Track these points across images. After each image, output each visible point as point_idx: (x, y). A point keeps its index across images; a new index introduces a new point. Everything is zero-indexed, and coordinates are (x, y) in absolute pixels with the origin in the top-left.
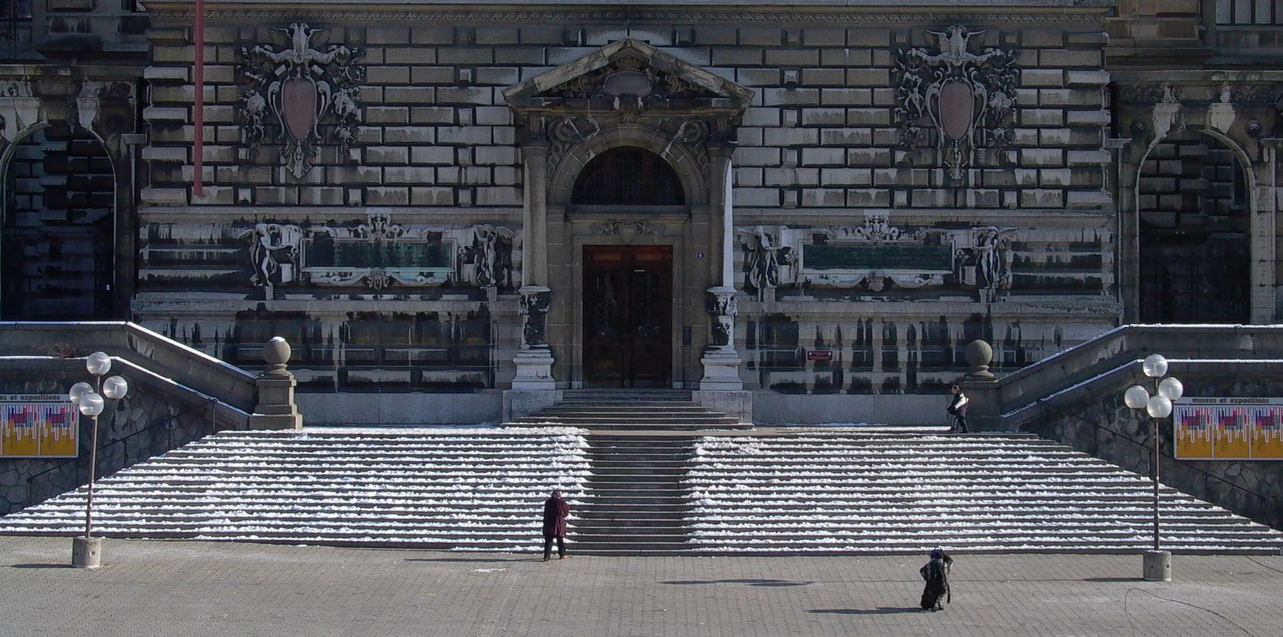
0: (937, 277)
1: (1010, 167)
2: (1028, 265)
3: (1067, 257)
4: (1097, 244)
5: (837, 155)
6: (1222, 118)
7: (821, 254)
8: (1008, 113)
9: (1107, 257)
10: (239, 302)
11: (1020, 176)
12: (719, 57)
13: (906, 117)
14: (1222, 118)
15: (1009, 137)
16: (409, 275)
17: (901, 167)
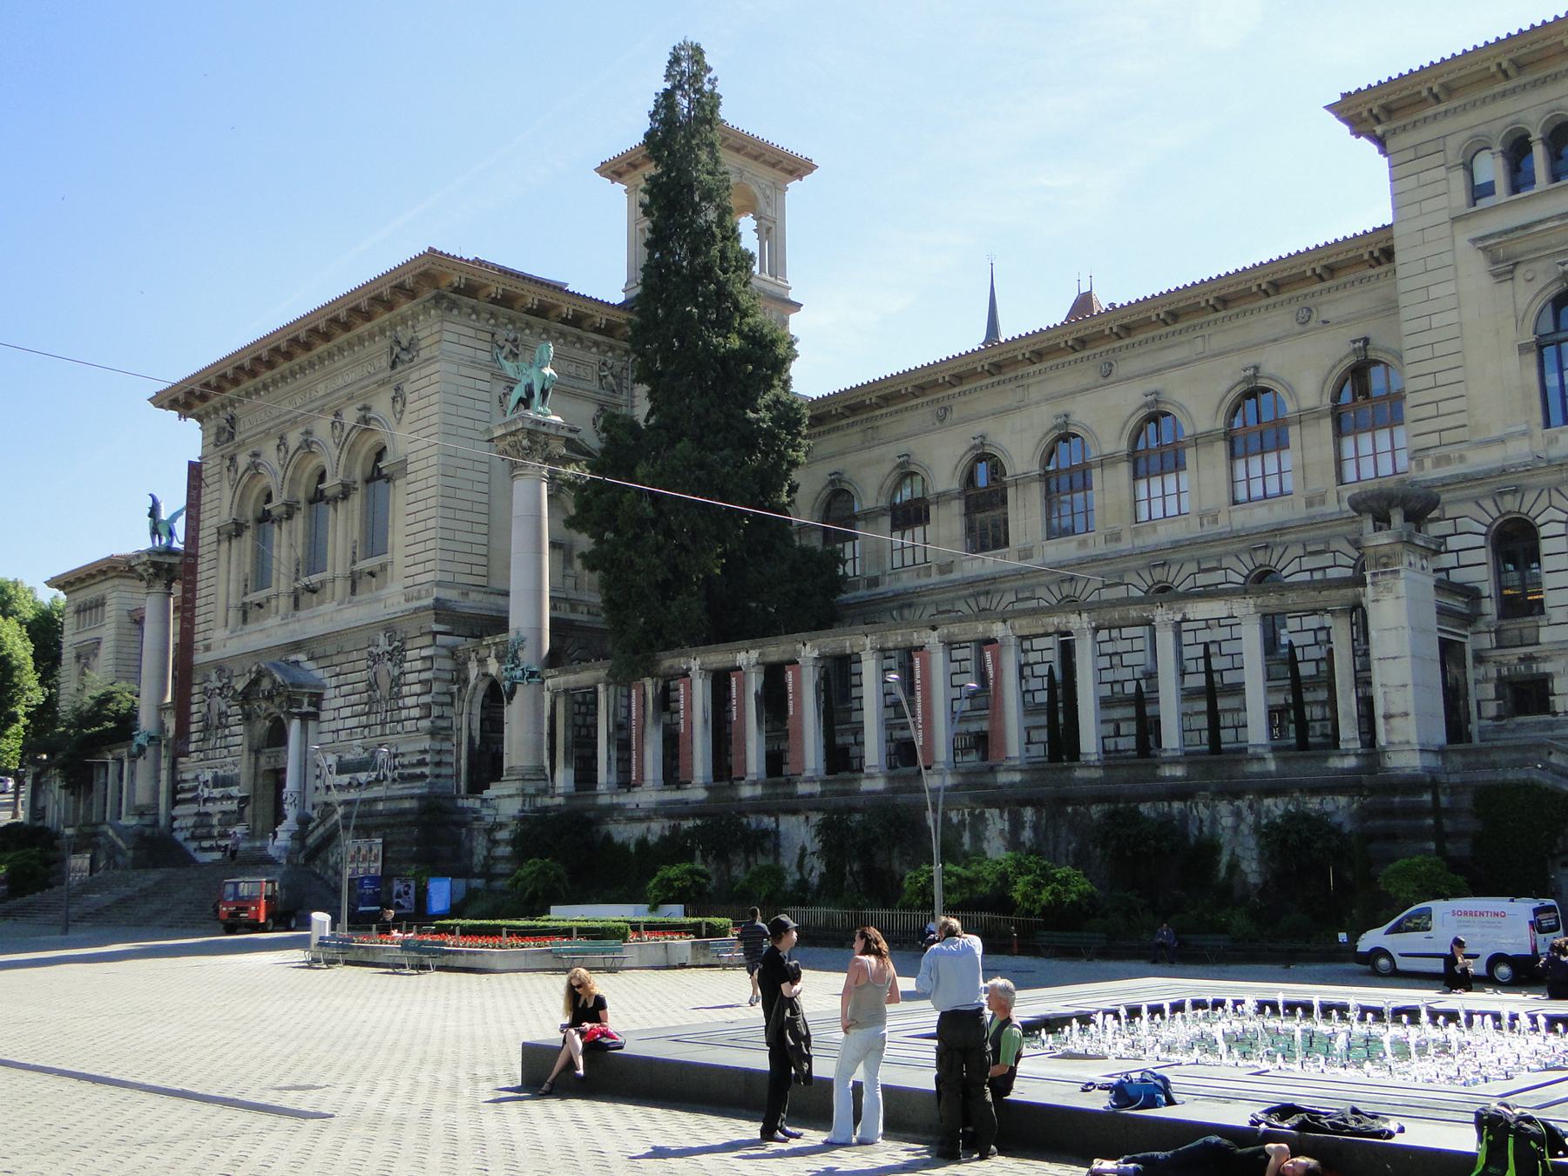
0: (374, 775)
1: (400, 709)
2: (403, 766)
3: (414, 759)
4: (425, 751)
5: (346, 712)
6: (493, 667)
7: (343, 768)
8: (399, 677)
9: (428, 758)
10: (193, 808)
11: (404, 713)
12: (323, 663)
13: (372, 685)
14: (493, 667)
15: (400, 691)
16: (234, 791)
17: (367, 714)
